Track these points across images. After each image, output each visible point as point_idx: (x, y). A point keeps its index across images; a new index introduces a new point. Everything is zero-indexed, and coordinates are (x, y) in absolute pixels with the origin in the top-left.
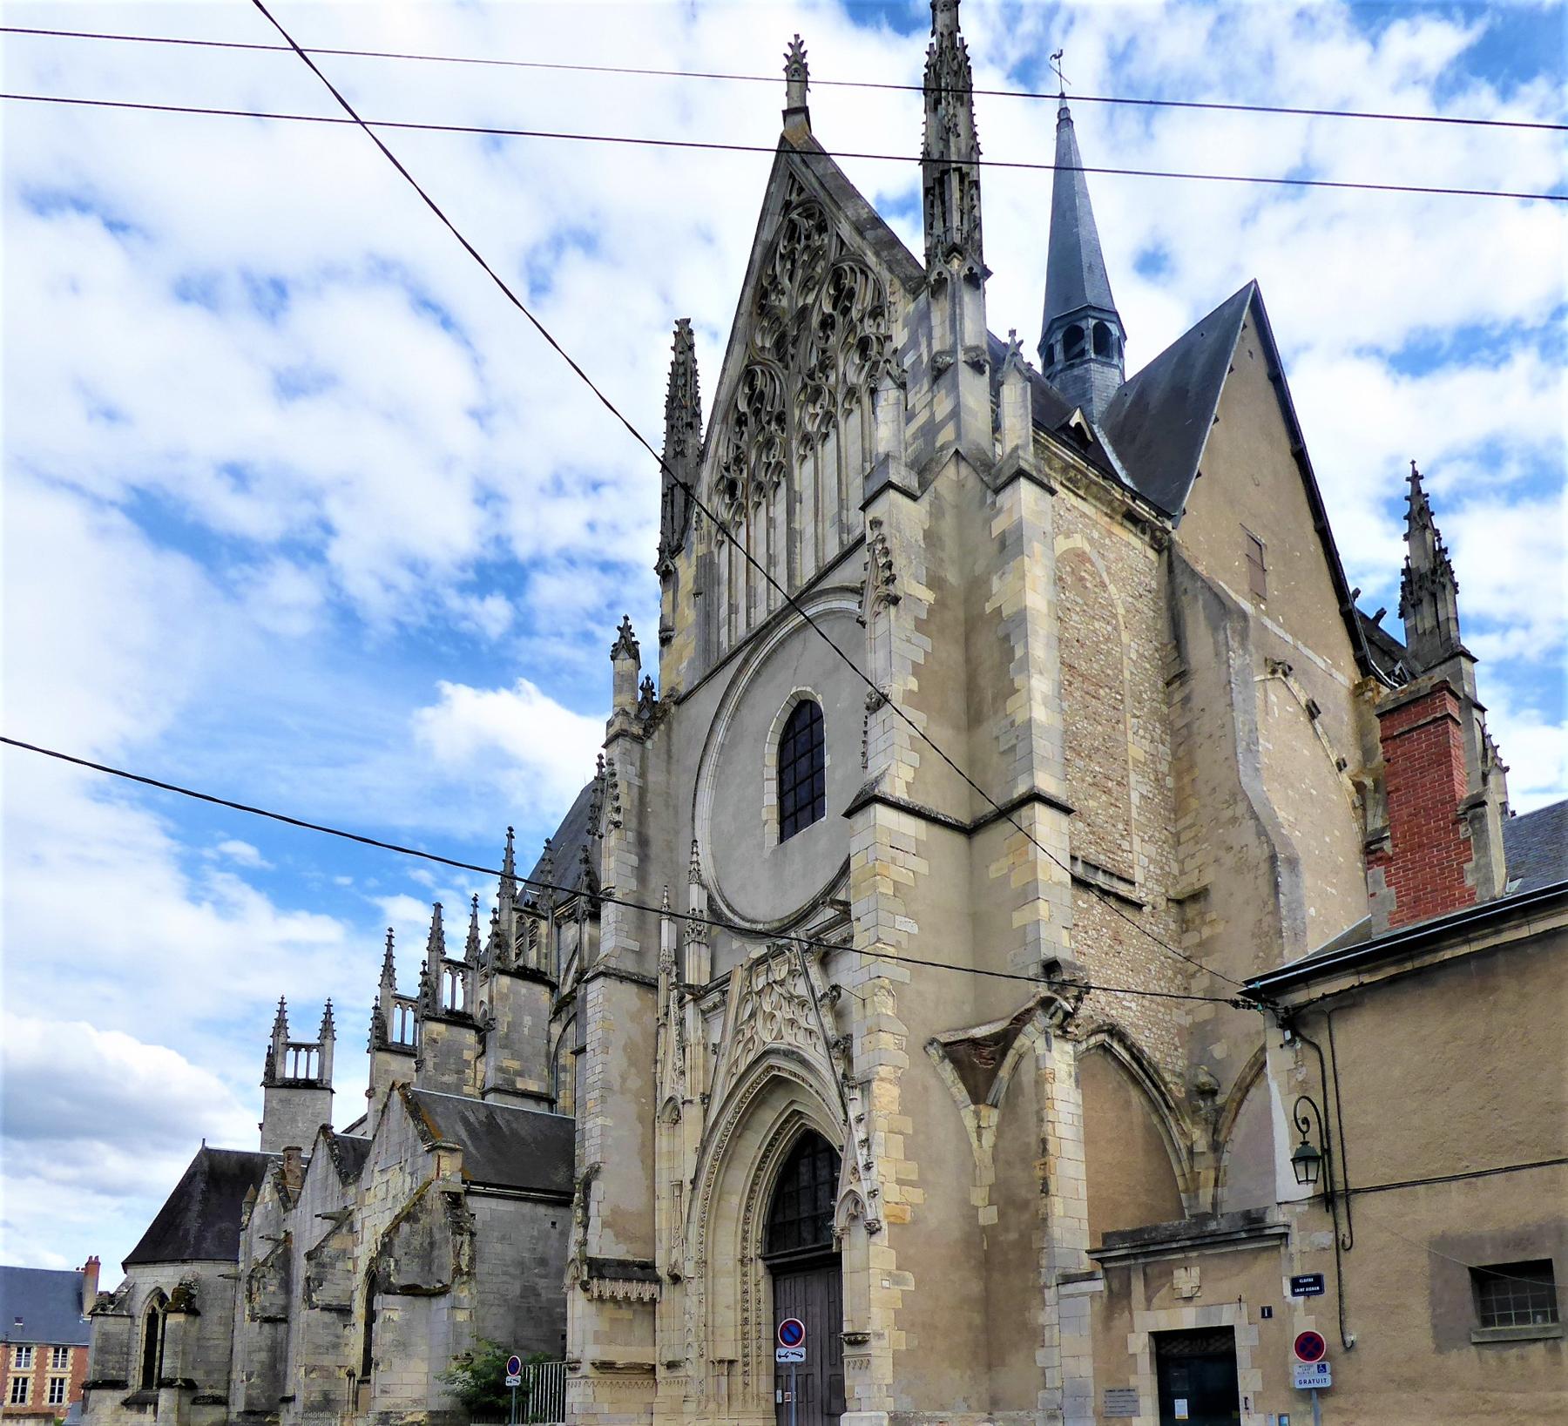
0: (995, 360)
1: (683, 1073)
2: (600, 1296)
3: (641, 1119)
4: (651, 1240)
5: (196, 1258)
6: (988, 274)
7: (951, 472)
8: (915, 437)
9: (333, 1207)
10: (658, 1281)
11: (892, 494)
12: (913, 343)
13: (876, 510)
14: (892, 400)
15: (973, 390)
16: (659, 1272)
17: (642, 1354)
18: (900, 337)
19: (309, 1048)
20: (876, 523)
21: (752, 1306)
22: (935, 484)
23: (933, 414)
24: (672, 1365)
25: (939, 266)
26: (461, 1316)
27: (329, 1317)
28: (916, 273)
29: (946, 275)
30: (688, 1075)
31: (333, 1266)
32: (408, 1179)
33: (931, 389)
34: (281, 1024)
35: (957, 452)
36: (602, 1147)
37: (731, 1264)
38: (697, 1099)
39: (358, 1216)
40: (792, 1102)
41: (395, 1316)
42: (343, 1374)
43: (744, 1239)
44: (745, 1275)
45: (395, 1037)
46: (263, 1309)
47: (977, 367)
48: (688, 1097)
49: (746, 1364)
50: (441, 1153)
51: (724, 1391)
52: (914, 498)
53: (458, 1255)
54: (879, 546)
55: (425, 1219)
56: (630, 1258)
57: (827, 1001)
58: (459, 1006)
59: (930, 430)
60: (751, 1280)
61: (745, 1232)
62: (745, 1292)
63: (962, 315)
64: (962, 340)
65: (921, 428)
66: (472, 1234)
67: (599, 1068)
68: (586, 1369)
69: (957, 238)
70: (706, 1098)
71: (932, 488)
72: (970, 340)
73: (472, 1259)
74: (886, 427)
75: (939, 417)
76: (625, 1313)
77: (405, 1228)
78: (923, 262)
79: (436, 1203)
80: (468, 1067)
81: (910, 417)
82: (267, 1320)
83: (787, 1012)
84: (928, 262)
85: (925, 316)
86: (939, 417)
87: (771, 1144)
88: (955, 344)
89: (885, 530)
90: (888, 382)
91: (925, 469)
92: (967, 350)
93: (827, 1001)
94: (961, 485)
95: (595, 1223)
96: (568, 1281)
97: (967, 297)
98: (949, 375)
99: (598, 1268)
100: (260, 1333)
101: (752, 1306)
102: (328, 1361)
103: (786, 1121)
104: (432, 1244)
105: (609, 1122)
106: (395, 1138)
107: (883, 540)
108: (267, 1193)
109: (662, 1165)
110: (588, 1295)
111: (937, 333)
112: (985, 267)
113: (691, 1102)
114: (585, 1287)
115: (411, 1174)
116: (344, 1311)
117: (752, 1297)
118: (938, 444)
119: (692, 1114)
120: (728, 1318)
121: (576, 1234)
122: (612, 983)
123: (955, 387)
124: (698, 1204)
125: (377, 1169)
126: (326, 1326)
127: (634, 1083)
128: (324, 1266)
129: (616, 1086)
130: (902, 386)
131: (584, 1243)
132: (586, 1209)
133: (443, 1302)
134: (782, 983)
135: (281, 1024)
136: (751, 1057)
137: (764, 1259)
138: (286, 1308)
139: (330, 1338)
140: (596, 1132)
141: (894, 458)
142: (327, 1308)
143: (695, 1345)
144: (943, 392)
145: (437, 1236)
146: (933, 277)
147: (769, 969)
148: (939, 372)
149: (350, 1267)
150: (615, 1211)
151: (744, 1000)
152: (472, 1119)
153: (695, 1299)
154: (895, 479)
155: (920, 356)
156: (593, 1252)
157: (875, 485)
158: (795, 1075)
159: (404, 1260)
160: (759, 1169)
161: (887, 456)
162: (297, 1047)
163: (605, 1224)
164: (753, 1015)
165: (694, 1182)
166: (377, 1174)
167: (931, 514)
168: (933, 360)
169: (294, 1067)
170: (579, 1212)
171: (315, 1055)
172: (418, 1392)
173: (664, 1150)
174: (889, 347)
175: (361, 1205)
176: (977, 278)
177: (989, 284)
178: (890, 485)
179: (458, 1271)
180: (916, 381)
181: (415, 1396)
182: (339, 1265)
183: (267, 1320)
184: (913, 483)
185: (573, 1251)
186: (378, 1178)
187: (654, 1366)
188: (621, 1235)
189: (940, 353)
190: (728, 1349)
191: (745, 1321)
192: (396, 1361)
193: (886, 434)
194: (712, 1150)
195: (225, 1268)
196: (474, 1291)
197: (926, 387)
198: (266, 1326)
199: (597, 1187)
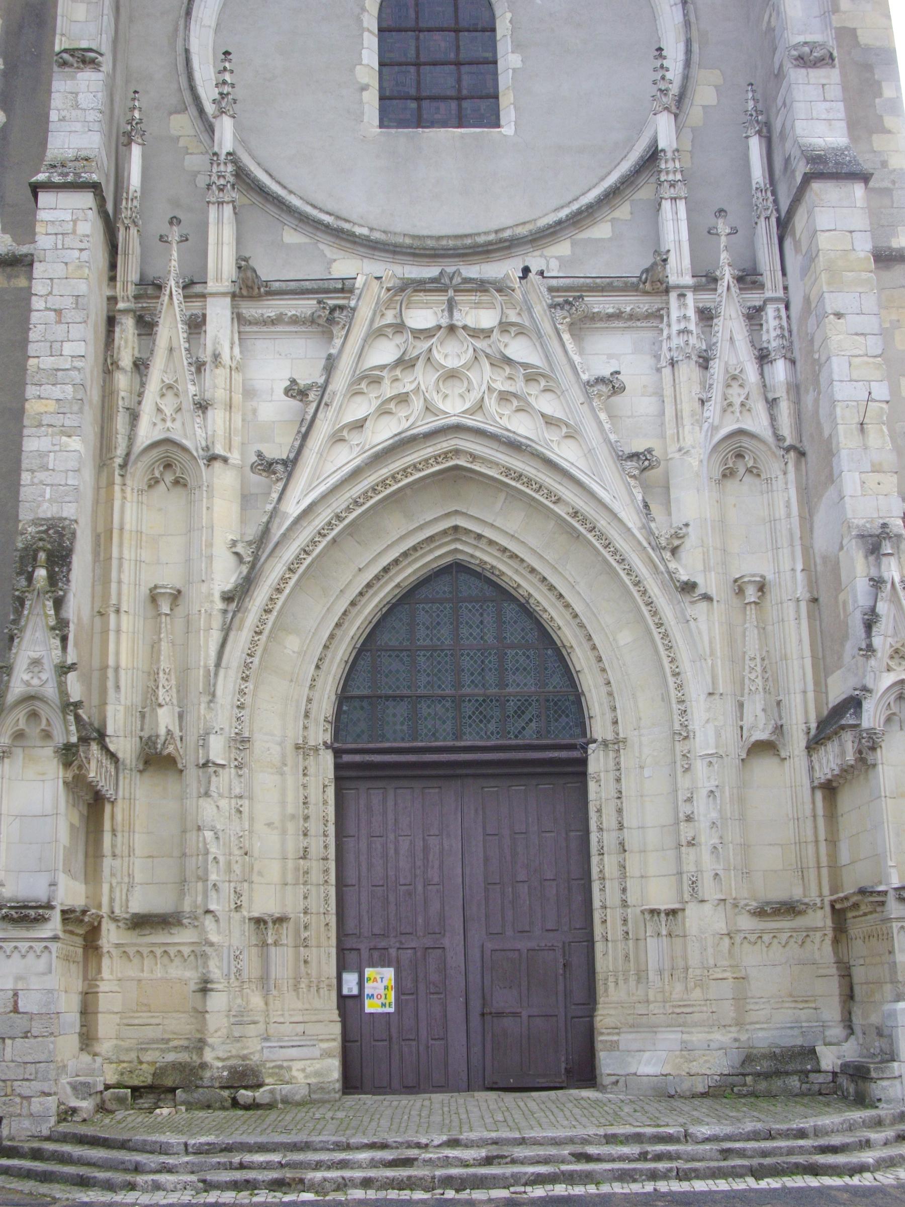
1: (202, 406)
24: (141, 922)
37: (276, 750)
40: (456, 512)
48: (219, 450)
87: (386, 570)
103: (431, 539)
113: (225, 460)
117: (312, 810)
119: (224, 483)
134: (477, 333)
147: (451, 306)
151: (377, 333)
158: (519, 477)
165: (235, 598)
191: (305, 855)
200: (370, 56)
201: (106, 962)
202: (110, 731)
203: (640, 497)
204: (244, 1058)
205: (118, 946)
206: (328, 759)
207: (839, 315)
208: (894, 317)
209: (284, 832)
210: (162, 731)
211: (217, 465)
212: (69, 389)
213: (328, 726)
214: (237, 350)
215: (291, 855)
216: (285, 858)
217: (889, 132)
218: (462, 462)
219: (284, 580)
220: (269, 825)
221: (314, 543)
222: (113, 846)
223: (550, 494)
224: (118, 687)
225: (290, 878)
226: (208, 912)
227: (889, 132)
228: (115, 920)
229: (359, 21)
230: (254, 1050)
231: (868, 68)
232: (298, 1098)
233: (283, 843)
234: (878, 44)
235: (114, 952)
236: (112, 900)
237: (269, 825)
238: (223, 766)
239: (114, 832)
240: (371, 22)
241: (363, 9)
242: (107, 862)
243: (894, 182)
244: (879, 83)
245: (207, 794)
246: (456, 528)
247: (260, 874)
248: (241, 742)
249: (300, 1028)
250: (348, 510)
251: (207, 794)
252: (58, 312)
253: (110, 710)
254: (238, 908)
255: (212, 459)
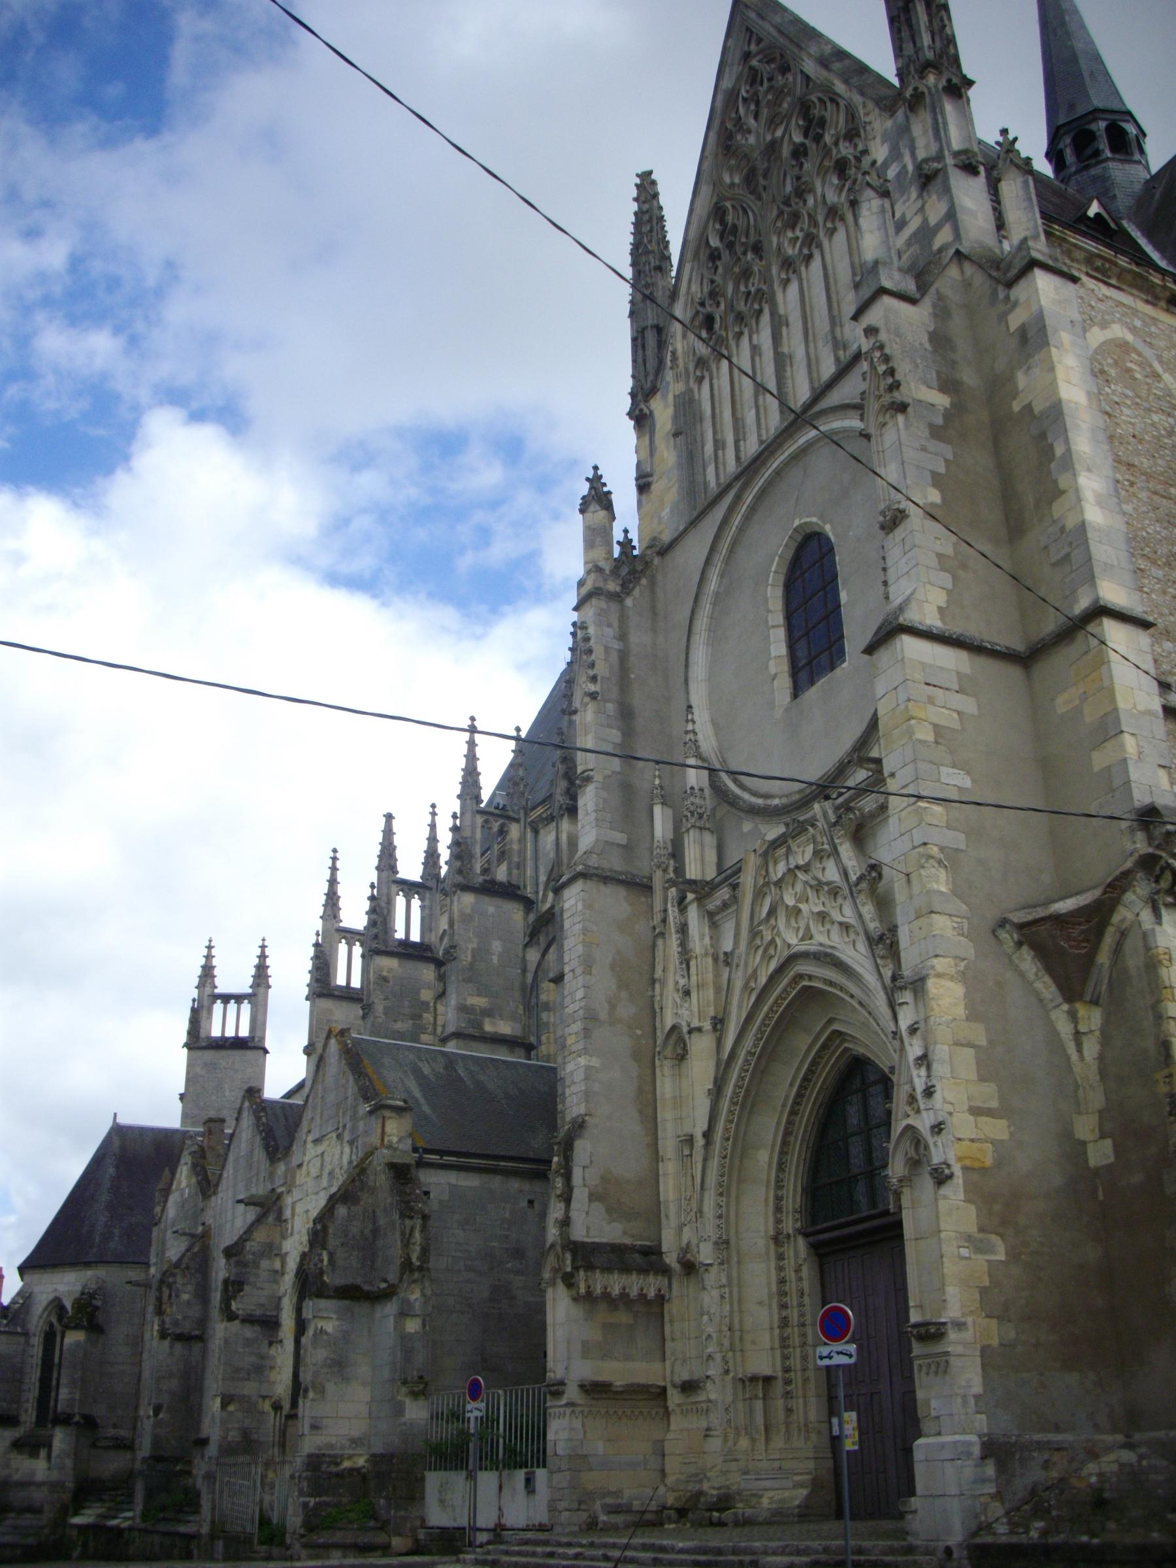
0: (995, 163)
1: (687, 993)
2: (589, 1293)
3: (636, 1056)
4: (654, 1214)
5: (100, 1262)
6: (970, 83)
7: (953, 272)
8: (909, 243)
9: (260, 1189)
10: (665, 1271)
11: (887, 300)
12: (895, 155)
13: (874, 316)
14: (875, 209)
15: (970, 195)
16: (667, 1261)
17: (644, 1371)
18: (880, 152)
19: (239, 998)
20: (871, 331)
21: (793, 1300)
22: (936, 285)
23: (925, 220)
24: (689, 1387)
25: (914, 83)
26: (412, 1326)
27: (249, 1332)
28: (889, 92)
29: (922, 88)
30: (694, 995)
31: (256, 1265)
32: (347, 1149)
33: (920, 196)
34: (207, 972)
35: (958, 252)
36: (588, 1095)
37: (761, 1242)
38: (707, 1025)
39: (289, 1200)
40: (831, 1021)
41: (329, 1327)
42: (267, 1406)
43: (778, 1209)
44: (780, 1257)
45: (341, 980)
46: (176, 1323)
47: (970, 169)
48: (695, 1023)
49: (788, 1382)
50: (387, 1113)
51: (759, 1419)
52: (912, 301)
53: (407, 1243)
54: (877, 354)
55: (366, 1199)
56: (627, 1241)
57: (864, 885)
58: (415, 937)
59: (926, 233)
60: (790, 1263)
61: (778, 1199)
62: (782, 1282)
63: (945, 123)
64: (949, 144)
65: (915, 234)
66: (425, 1218)
67: (580, 994)
68: (572, 1392)
69: (930, 55)
70: (719, 1023)
71: (933, 290)
72: (956, 145)
73: (425, 1251)
74: (872, 234)
75: (933, 220)
76: (623, 1317)
77: (342, 1211)
78: (895, 82)
79: (381, 1180)
80: (427, 1010)
81: (900, 225)
82: (180, 1338)
83: (815, 905)
84: (901, 80)
85: (905, 130)
86: (933, 220)
87: (806, 1079)
88: (941, 149)
89: (883, 336)
90: (869, 193)
91: (923, 275)
92: (956, 154)
93: (864, 885)
94: (967, 285)
95: (580, 1195)
96: (547, 1275)
97: (949, 107)
98: (939, 179)
99: (586, 1256)
100: (171, 1354)
101: (793, 1300)
102: (249, 1388)
103: (824, 1047)
104: (376, 1232)
105: (595, 1062)
106: (331, 1098)
107: (881, 347)
108: (184, 1177)
109: (666, 1114)
110: (574, 1293)
111: (920, 143)
112: (965, 77)
113: (699, 1030)
114: (569, 1281)
115: (351, 1143)
116: (270, 1324)
117: (792, 1287)
118: (936, 247)
119: (701, 1048)
120: (761, 1318)
121: (556, 1211)
122: (590, 885)
123: (947, 190)
124: (714, 1163)
125: (310, 1138)
126: (248, 1343)
127: (626, 1011)
128: (245, 1265)
129: (603, 1016)
130: (885, 194)
131: (566, 1223)
132: (568, 1177)
133: (391, 1308)
134: (806, 868)
135: (207, 972)
136: (773, 965)
137: (806, 1235)
138: (203, 1321)
139: (252, 1359)
140: (579, 1076)
141: (885, 264)
142: (249, 1320)
143: (718, 1357)
144: (934, 197)
145: (382, 1221)
146: (908, 93)
148: (928, 178)
149: (277, 1265)
150: (605, 1179)
152: (426, 1070)
153: (715, 1293)
154: (887, 284)
155: (905, 166)
156: (579, 1233)
157: (866, 292)
159: (340, 1254)
160: (793, 1112)
161: (876, 263)
162: (226, 998)
163: (593, 1197)
164: (772, 912)
165: (707, 1135)
166: (310, 1145)
167: (935, 315)
168: (919, 167)
169: (228, 1022)
170: (559, 1183)
171: (246, 1007)
172: (358, 1429)
173: (668, 1095)
174: (866, 161)
175: (290, 1184)
176: (958, 88)
177: (972, 93)
178: (883, 291)
179: (407, 1266)
180: (903, 190)
181: (356, 1433)
182: (265, 1264)
183: (180, 1338)
184: (910, 286)
185: (552, 1233)
186: (312, 1151)
187: (664, 1389)
188: (615, 1211)
189: (926, 161)
190: (762, 1362)
191: (784, 1323)
192: (330, 1387)
193: (871, 244)
194: (729, 1090)
195: (135, 1274)
196: (428, 1292)
197: (914, 195)
198: (178, 1346)
199: (583, 1149)
200: (778, 646)
201: (673, 1418)
202: (664, 1249)
203: (890, 973)
204: (728, 1487)
205: (679, 1405)
206: (801, 1242)
207: (892, 775)
208: (1082, 691)
209: (770, 1307)
210: (685, 1241)
211: (695, 1035)
212: (579, 1023)
213: (798, 1216)
214: (707, 940)
215: (776, 1324)
216: (772, 1328)
217: (1064, 492)
218: (806, 983)
219: (731, 1112)
220: (760, 1303)
221: (743, 1079)
222: (672, 1332)
223: (847, 992)
224: (667, 1216)
225: (777, 1345)
226: (708, 1377)
227: (1064, 492)
228: (674, 1386)
229: (767, 621)
230: (735, 1481)
231: (1043, 436)
232: (760, 1519)
233: (771, 1315)
234: (1048, 404)
235: (678, 1410)
236: (672, 1372)
237: (760, 1303)
238: (711, 1265)
239: (671, 1321)
240: (777, 617)
241: (769, 611)
242: (669, 1345)
243: (1071, 544)
244: (1052, 445)
245: (704, 1288)
246: (835, 1032)
247: (753, 1343)
248: (723, 1244)
249: (776, 1464)
250: (756, 1046)
251: (704, 1288)
252: (573, 971)
253: (664, 1233)
254: (727, 1372)
255: (690, 1032)
